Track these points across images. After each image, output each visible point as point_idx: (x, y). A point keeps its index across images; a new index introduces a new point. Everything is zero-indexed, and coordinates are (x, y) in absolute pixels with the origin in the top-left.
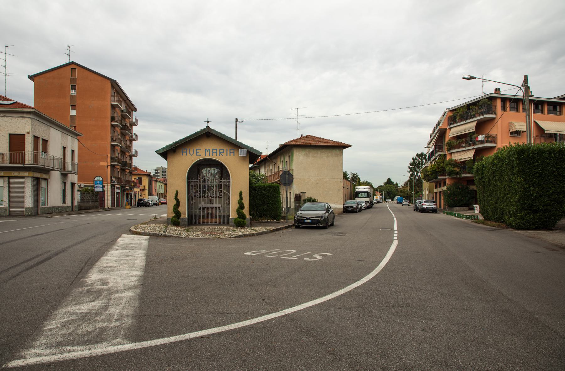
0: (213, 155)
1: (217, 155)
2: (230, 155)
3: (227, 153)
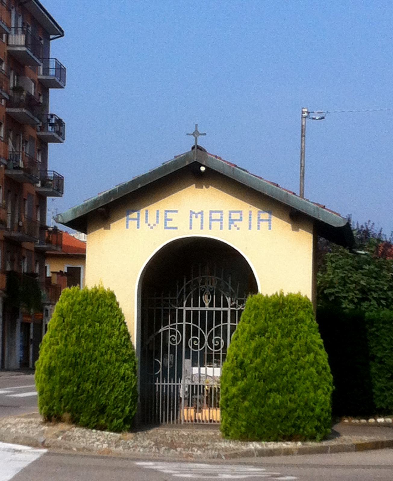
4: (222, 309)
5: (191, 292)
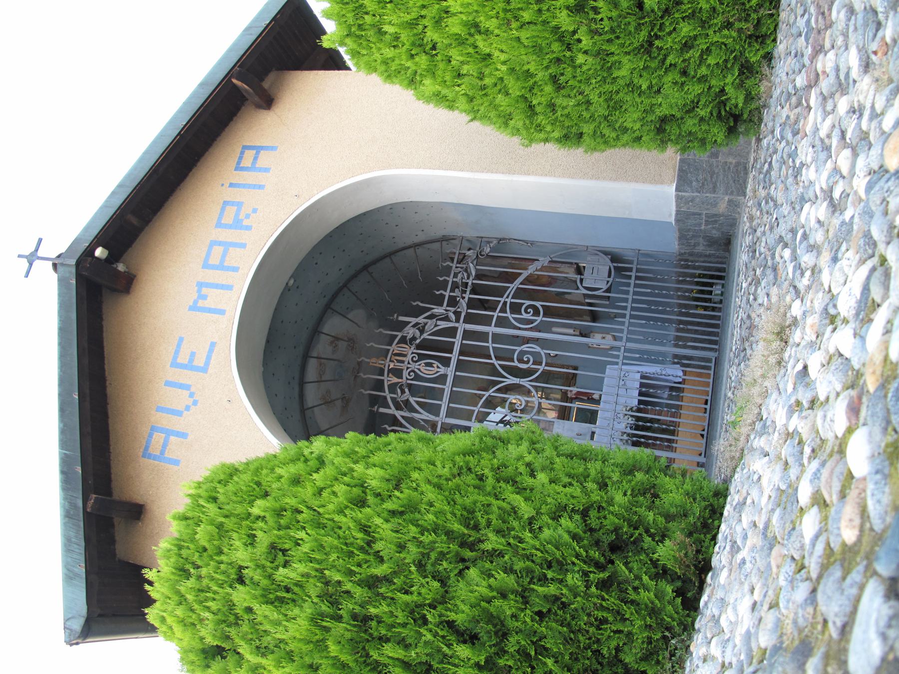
1: (243, 246)
3: (249, 186)
4: (458, 341)
5: (412, 400)
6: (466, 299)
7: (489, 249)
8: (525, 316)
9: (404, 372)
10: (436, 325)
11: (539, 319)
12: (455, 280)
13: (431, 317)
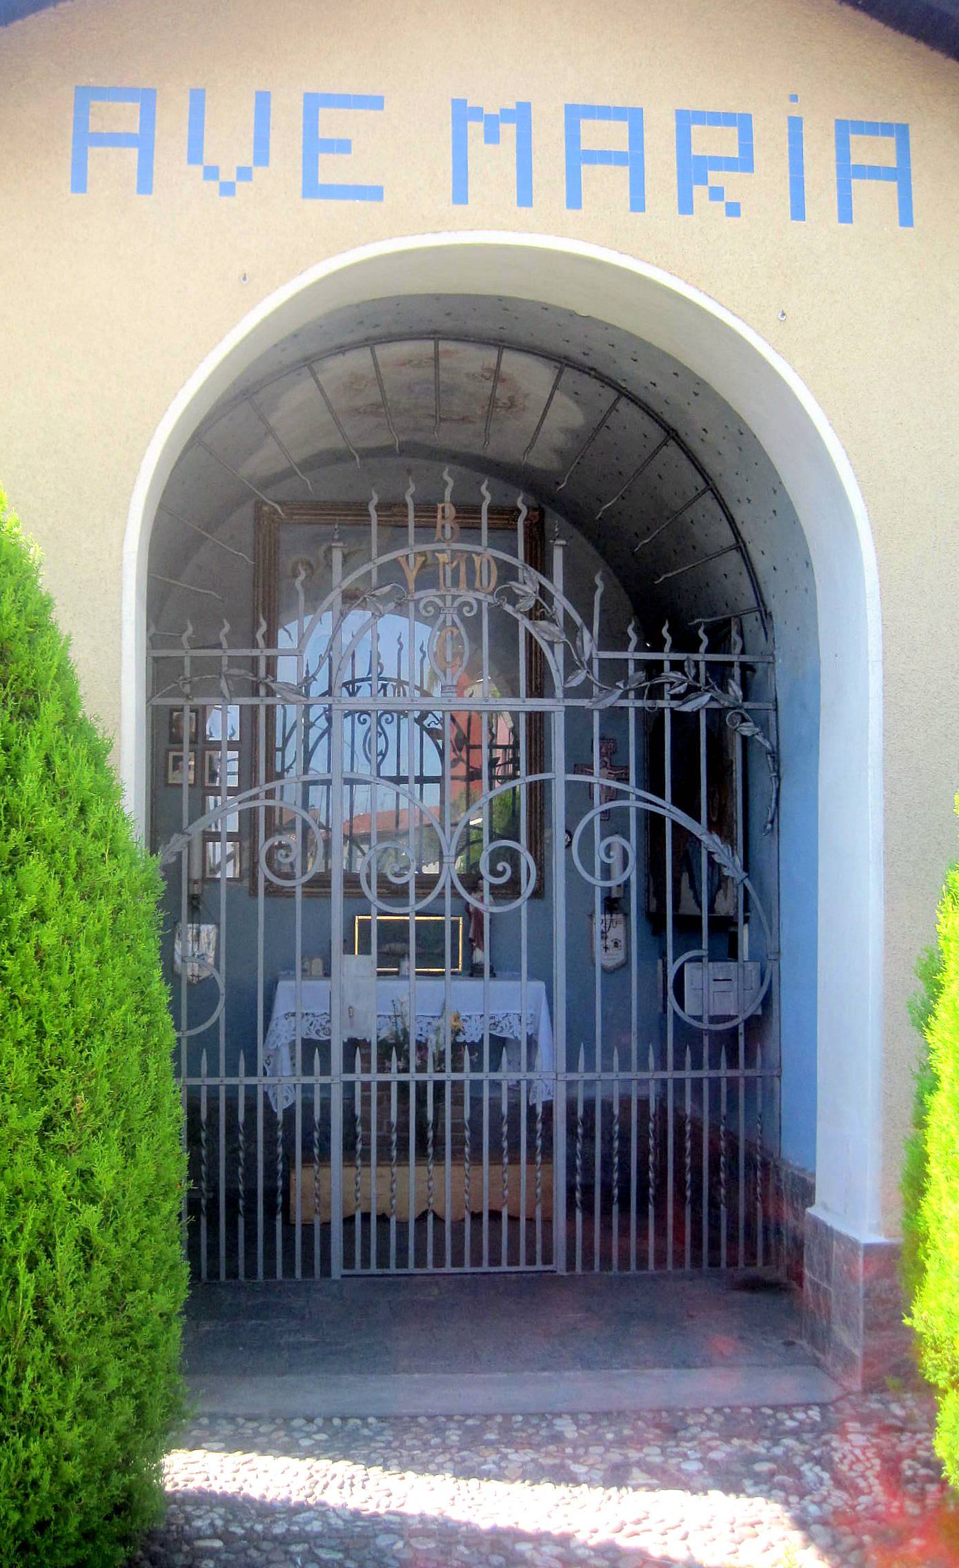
0: (574, 200)
1: (638, 204)
2: (846, 215)
6: (623, 703)
7: (747, 733)
8: (600, 846)
9: (433, 592)
10: (551, 645)
11: (598, 882)
12: (667, 665)
13: (571, 629)
